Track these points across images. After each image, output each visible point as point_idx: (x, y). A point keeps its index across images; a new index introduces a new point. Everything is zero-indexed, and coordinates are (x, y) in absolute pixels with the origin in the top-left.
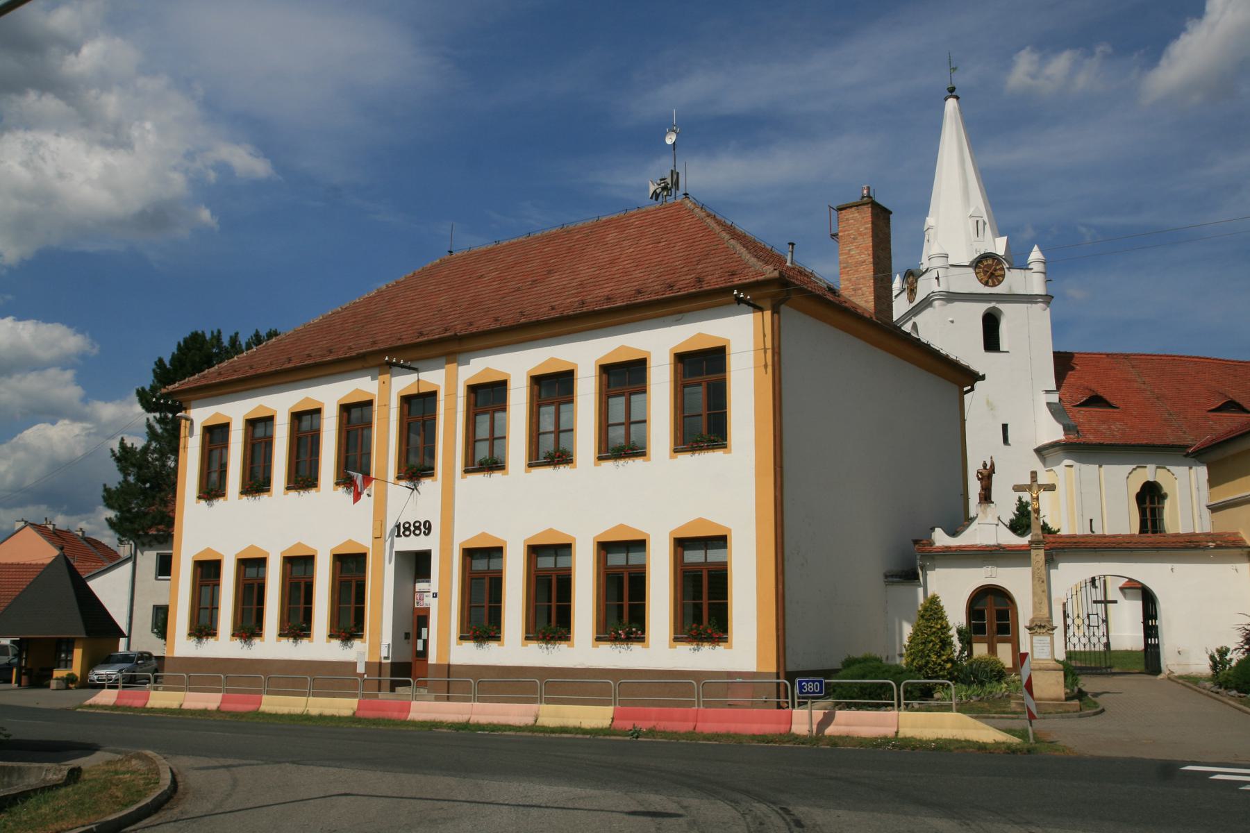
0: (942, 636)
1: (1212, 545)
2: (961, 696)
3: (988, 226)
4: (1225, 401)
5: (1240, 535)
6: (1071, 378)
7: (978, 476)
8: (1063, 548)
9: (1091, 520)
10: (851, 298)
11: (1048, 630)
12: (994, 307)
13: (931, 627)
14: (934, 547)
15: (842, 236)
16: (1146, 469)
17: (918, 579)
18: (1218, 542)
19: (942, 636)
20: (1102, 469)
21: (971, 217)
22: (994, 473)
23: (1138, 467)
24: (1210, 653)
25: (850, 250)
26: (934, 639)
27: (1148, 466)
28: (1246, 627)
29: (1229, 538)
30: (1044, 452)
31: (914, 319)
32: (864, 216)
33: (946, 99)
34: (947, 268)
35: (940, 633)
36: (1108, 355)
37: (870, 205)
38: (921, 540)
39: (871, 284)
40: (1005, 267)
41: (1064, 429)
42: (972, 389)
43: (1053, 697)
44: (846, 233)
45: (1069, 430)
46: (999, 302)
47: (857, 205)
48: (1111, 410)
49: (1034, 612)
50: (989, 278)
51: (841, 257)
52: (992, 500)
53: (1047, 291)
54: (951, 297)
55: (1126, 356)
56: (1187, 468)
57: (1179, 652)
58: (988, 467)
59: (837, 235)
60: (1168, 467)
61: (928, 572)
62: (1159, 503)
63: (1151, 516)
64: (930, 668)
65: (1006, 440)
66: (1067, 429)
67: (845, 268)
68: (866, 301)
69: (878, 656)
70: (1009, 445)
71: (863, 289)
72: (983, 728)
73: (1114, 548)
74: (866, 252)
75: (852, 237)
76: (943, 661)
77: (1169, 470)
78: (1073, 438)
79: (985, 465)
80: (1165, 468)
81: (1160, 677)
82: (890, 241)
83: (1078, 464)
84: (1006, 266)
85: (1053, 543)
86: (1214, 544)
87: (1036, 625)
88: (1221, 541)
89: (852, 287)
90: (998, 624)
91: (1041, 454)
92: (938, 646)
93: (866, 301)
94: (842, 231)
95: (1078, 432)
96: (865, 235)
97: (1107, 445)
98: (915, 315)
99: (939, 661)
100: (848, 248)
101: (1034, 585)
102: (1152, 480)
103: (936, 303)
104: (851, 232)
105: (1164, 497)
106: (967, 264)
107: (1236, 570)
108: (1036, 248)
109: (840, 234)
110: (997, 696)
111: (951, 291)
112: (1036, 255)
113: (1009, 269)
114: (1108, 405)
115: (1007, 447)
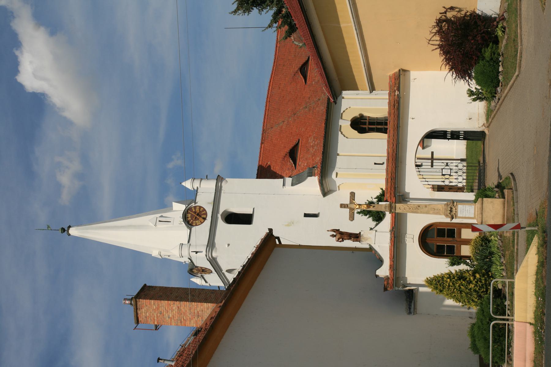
0: (456, 278)
1: (397, 93)
2: (501, 269)
3: (164, 215)
4: (300, 74)
5: (391, 75)
6: (276, 168)
7: (340, 241)
8: (395, 188)
9: (375, 164)
10: (204, 320)
11: (453, 206)
12: (222, 215)
13: (449, 286)
14: (389, 276)
15: (158, 322)
17: (412, 290)
18: (395, 89)
19: (456, 278)
20: (340, 154)
21: (156, 225)
22: (339, 230)
23: (340, 131)
24: (471, 101)
25: (169, 317)
26: (458, 285)
27: (340, 124)
28: (454, 78)
29: (393, 81)
30: (326, 191)
31: (224, 271)
32: (145, 305)
33: (69, 235)
34: (190, 245)
35: (454, 280)
36: (262, 143)
37: (138, 300)
38: (385, 285)
39: (195, 304)
40: (194, 206)
41: (311, 176)
42: (278, 238)
43: (502, 207)
44: (155, 318)
45: (312, 173)
46: (218, 212)
47: (136, 309)
48: (300, 144)
49: (440, 214)
50: (200, 216)
51: (173, 324)
52: (358, 233)
53: (214, 179)
54: (211, 244)
55: (264, 131)
56: (343, 99)
57: (470, 119)
58: (335, 234)
59: (156, 325)
60: (342, 112)
61: (408, 282)
62: (366, 120)
63: (374, 125)
64: (479, 289)
65: (316, 216)
66: (311, 174)
67: (181, 322)
68: (208, 309)
69: (470, 326)
70: (319, 213)
71: (198, 310)
72: (527, 261)
73: (396, 154)
74: (172, 305)
75: (159, 314)
76: (474, 280)
77: (344, 111)
78: (317, 171)
79: (333, 236)
80: (342, 114)
81: (486, 132)
82: (166, 287)
83: (336, 169)
84: (193, 205)
85: (391, 194)
86: (397, 91)
87: (450, 213)
88: (395, 87)
89: (196, 318)
90: (447, 237)
91: (327, 193)
92: (463, 282)
93: (208, 309)
94: (154, 322)
95: (314, 167)
96: (159, 305)
97: (324, 149)
98: (221, 270)
99: (474, 282)
100: (167, 318)
101: (421, 213)
102: (350, 123)
103: (214, 255)
104: (155, 315)
105: (362, 116)
106: (189, 231)
107: (414, 79)
108: (183, 184)
109: (156, 323)
110: (501, 244)
111: (207, 244)
112: (188, 184)
113: (195, 203)
114: (296, 145)
115: (320, 215)
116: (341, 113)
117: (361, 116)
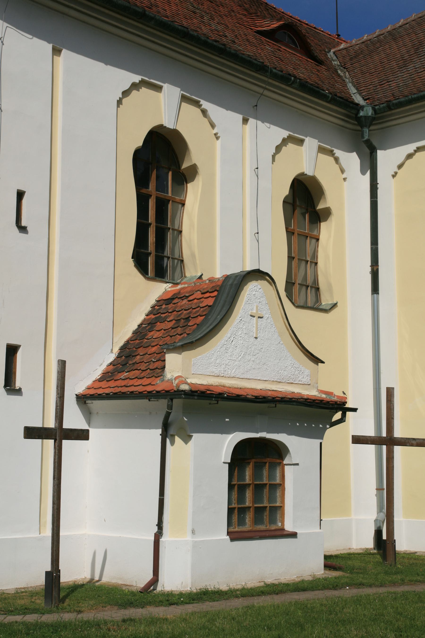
9: (20, 195)
16: (161, 95)
27: (166, 86)
60: (205, 104)
77: (204, 112)
80: (197, 104)
102: (169, 124)
116: (202, 102)
117: (183, 175)
